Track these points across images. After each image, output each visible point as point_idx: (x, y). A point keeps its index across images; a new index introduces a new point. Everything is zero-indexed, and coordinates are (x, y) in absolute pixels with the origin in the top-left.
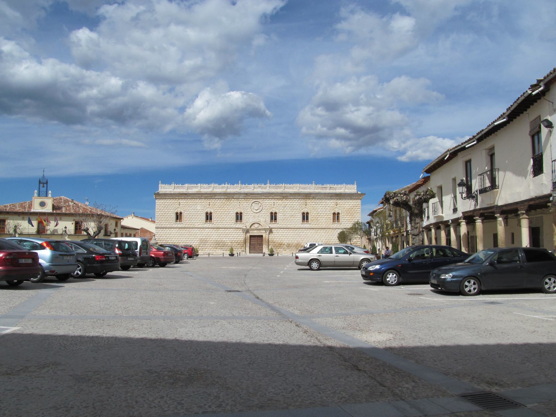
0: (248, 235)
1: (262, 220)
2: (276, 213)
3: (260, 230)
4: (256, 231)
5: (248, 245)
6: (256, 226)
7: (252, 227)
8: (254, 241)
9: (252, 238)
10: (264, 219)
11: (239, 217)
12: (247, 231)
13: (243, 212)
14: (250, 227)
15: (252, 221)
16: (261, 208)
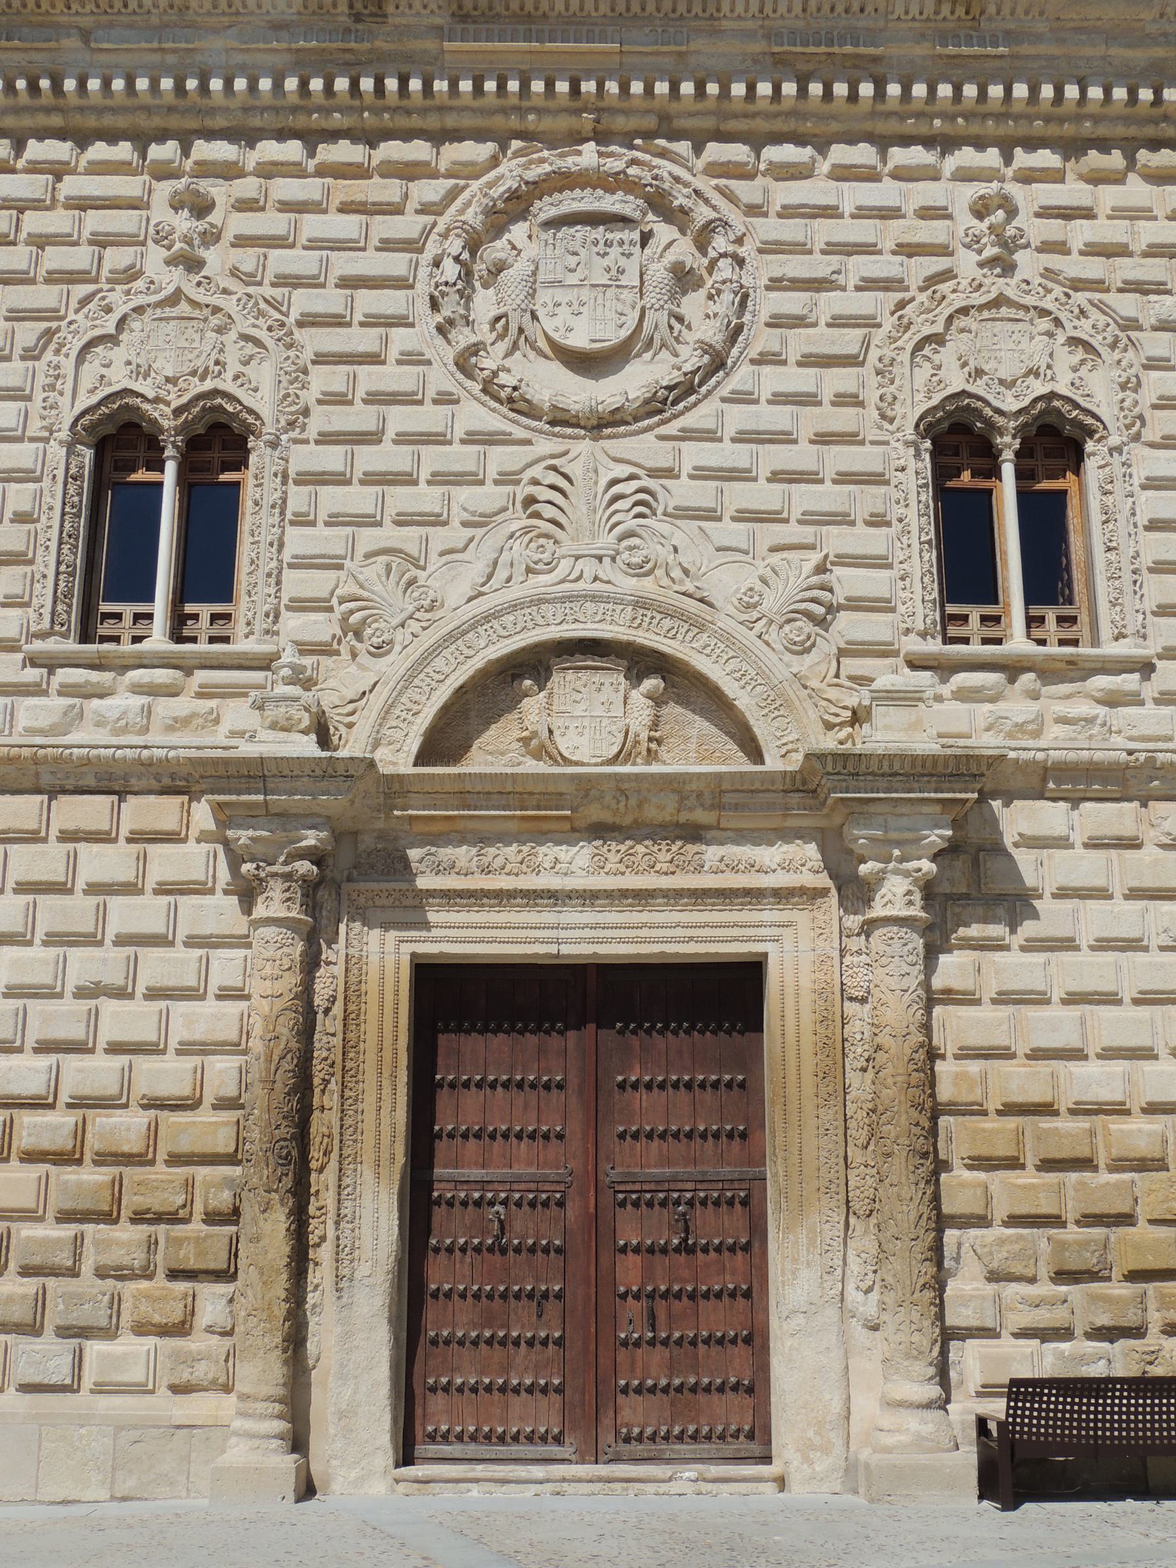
0: (378, 958)
1: (726, 583)
2: (1056, 440)
3: (687, 817)
4: (574, 864)
5: (366, 1218)
6: (587, 723)
7: (495, 753)
8: (523, 1123)
9: (471, 1053)
10: (789, 574)
11: (159, 506)
12: (339, 849)
13: (260, 394)
14: (444, 741)
15: (478, 591)
16: (703, 317)
